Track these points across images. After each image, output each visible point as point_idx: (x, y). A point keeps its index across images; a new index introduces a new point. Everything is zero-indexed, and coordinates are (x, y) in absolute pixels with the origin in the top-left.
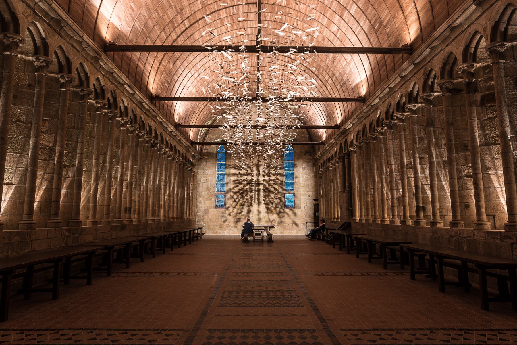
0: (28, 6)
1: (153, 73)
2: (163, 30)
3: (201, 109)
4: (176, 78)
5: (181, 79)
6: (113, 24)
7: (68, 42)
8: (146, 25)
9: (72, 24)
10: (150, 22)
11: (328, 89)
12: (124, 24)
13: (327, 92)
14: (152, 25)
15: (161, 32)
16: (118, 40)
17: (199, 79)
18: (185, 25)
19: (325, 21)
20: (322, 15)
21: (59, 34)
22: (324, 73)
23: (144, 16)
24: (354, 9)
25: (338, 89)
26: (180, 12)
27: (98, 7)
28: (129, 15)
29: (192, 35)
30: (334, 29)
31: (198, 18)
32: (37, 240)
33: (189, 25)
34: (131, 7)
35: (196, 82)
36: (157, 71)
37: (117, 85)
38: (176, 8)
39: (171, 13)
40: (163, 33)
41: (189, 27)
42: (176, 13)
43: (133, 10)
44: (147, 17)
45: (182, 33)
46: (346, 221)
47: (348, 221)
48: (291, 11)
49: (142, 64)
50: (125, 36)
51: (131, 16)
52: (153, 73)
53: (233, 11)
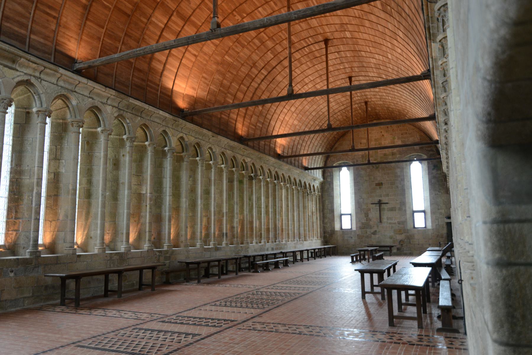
0: (113, 106)
1: (240, 119)
2: (242, 83)
4: (269, 117)
5: (276, 116)
6: (188, 95)
7: (148, 120)
8: (222, 85)
9: (147, 108)
10: (225, 82)
12: (199, 91)
14: (228, 84)
15: (240, 85)
16: (196, 104)
17: (297, 112)
18: (262, 74)
19: (389, 45)
20: (384, 41)
21: (141, 117)
23: (218, 79)
24: (401, 34)
26: (254, 65)
27: (171, 87)
28: (202, 83)
29: (274, 79)
30: (399, 51)
31: (274, 65)
32: (133, 258)
33: (267, 73)
34: (203, 77)
36: (245, 117)
37: (201, 138)
38: (248, 64)
39: (245, 70)
40: (242, 86)
41: (268, 74)
42: (250, 68)
43: (206, 79)
44: (221, 79)
45: (262, 81)
48: (359, 40)
49: (225, 115)
50: (203, 99)
51: (205, 83)
52: (240, 119)
53: (306, 51)
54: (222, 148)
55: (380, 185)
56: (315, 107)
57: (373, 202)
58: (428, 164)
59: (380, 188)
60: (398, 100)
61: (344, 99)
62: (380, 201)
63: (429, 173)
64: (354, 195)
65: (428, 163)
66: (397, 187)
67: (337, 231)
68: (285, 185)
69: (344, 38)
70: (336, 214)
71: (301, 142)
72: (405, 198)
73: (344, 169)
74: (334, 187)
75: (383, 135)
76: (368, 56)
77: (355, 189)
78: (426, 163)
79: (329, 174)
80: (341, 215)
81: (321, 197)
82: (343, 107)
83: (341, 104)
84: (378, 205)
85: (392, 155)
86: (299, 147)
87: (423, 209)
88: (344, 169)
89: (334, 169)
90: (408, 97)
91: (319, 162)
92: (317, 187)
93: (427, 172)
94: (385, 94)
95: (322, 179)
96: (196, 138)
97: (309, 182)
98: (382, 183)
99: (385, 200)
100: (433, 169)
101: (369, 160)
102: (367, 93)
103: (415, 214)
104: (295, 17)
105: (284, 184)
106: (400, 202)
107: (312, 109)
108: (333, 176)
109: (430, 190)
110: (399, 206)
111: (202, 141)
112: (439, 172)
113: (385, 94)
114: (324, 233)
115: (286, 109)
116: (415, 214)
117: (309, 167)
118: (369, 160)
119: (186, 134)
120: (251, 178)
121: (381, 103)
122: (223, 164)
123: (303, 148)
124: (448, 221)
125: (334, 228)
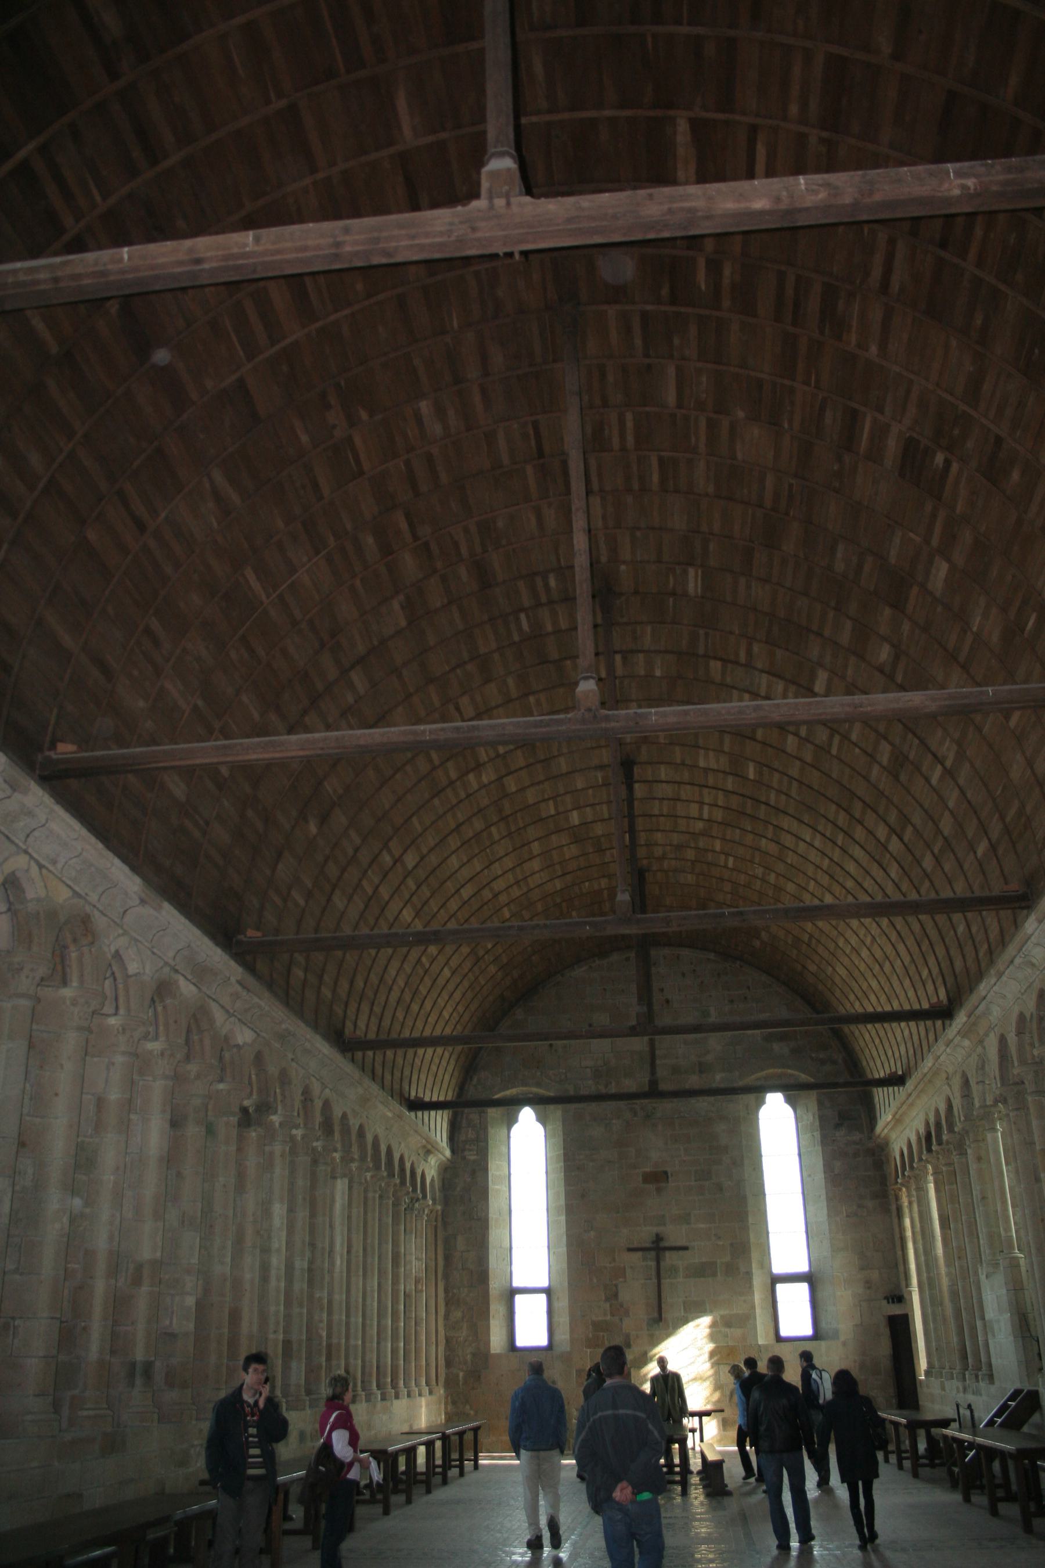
3: (441, 981)
11: (893, 875)
13: (890, 889)
22: (870, 818)
25: (929, 870)
30: (884, 654)
35: (411, 883)
46: (1018, 1386)
47: (1027, 1387)
53: (520, 629)
54: (166, 964)
55: (658, 1178)
56: (477, 865)
57: (636, 1245)
58: (819, 1109)
59: (659, 1190)
60: (759, 871)
61: (573, 850)
62: (659, 1238)
63: (825, 1141)
64: (563, 1218)
65: (820, 1104)
66: (720, 1188)
67: (499, 1355)
68: (347, 1159)
69: (674, 594)
70: (495, 1285)
71: (407, 997)
72: (745, 1228)
73: (527, 1115)
74: (491, 1186)
75: (667, 1001)
76: (728, 680)
77: (568, 1195)
78: (811, 1099)
79: (471, 1134)
80: (513, 1292)
81: (440, 1219)
82: (558, 885)
83: (557, 867)
84: (653, 1254)
85: (701, 1072)
86: (400, 1015)
87: (803, 1267)
88: (527, 1115)
89: (492, 1112)
90: (814, 855)
91: (445, 1086)
92: (432, 1180)
93: (817, 1135)
94: (718, 845)
95: (448, 1153)
96: (76, 894)
97: (413, 1158)
98: (666, 1173)
99: (675, 1235)
100: (838, 1126)
101: (653, 1083)
102: (659, 837)
103: (780, 1288)
104: (964, 187)
105: (342, 1158)
106: (732, 1245)
107: (466, 873)
108: (486, 1141)
109: (829, 1200)
110: (727, 1258)
111: (96, 913)
112: (857, 1136)
113: (718, 845)
114: (449, 1364)
115: (390, 852)
116: (780, 1288)
117: (427, 1099)
118: (653, 1083)
119: (41, 867)
120: (246, 1119)
121: (690, 878)
122: (156, 1038)
123: (409, 1023)
124: (896, 1310)
125: (488, 1343)
